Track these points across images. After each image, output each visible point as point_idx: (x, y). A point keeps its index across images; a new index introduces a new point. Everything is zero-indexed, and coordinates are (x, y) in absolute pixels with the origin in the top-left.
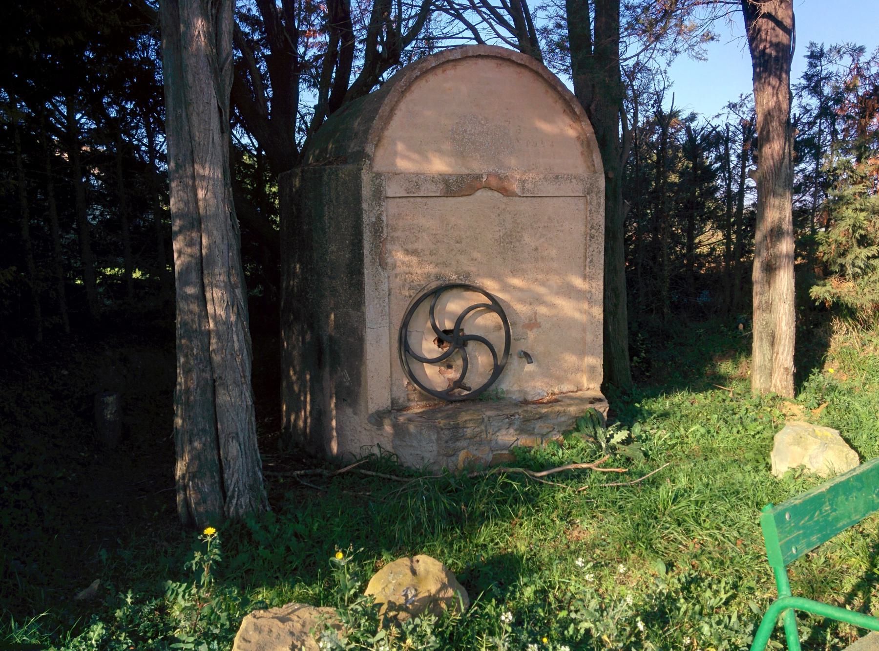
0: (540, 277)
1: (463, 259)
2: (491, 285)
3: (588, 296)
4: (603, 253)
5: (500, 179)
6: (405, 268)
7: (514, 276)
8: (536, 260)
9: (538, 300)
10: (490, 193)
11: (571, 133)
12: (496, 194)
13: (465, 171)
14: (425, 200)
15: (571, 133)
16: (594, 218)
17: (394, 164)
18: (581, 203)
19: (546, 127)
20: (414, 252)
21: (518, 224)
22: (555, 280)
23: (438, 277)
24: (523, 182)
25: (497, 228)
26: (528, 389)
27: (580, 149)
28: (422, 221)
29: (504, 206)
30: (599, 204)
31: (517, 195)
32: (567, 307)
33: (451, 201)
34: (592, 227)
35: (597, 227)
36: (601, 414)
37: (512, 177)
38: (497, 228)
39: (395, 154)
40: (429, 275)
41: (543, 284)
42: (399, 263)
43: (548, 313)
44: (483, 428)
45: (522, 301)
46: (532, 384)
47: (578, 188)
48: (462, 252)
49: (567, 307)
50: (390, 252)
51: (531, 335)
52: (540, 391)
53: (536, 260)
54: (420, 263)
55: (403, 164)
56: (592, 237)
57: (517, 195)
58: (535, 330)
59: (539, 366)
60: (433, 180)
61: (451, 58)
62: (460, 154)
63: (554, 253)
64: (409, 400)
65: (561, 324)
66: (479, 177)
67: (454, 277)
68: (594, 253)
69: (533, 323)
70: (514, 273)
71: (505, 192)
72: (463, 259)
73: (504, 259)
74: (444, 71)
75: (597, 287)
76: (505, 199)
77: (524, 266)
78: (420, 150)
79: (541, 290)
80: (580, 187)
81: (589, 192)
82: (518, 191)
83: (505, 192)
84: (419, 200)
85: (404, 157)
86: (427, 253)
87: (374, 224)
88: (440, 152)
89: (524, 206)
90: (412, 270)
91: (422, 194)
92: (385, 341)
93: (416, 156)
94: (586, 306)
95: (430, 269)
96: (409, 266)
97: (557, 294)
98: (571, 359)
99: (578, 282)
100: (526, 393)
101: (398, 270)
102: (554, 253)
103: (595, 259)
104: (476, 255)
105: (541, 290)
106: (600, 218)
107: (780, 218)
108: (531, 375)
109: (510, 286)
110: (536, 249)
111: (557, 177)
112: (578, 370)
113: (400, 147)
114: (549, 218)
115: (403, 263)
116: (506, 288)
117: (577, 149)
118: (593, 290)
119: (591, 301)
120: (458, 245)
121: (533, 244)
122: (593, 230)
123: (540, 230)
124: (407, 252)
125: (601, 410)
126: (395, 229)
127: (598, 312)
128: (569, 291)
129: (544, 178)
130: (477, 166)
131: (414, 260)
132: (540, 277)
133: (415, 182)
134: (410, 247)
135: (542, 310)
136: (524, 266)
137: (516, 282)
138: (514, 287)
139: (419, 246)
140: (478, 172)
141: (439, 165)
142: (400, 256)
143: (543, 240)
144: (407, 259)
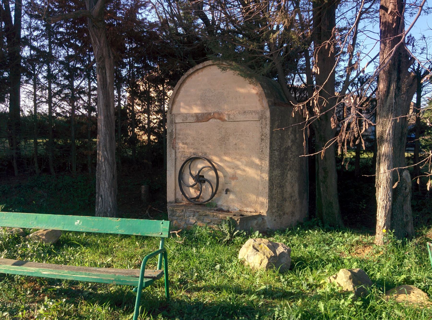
0: (238, 157)
1: (204, 147)
2: (215, 159)
3: (260, 168)
4: (268, 148)
5: (219, 114)
6: (182, 150)
7: (225, 156)
8: (236, 149)
9: (237, 167)
10: (216, 120)
11: (254, 91)
12: (218, 120)
13: (205, 112)
14: (190, 124)
15: (254, 91)
16: (264, 130)
17: (180, 111)
18: (258, 124)
19: (242, 90)
20: (186, 144)
21: (227, 133)
22: (244, 159)
23: (194, 154)
24: (229, 115)
25: (218, 135)
26: (231, 206)
27: (258, 98)
28: (188, 132)
29: (221, 126)
30: (266, 124)
31: (226, 121)
32: (251, 172)
33: (200, 124)
34: (262, 135)
35: (265, 135)
36: (236, 221)
37: (224, 113)
38: (218, 135)
39: (180, 107)
40: (191, 153)
41: (239, 160)
42: (180, 148)
43: (241, 174)
44: (183, 214)
45: (229, 167)
46: (233, 204)
47: (256, 117)
48: (203, 144)
49: (251, 172)
50: (178, 143)
51: (233, 183)
52: (236, 208)
53: (236, 149)
54: (188, 148)
55: (183, 111)
56: (262, 140)
57: (226, 121)
58: (235, 180)
59: (236, 196)
60: (192, 116)
61: (198, 68)
62: (204, 105)
63: (244, 146)
64: (183, 200)
65: (247, 179)
66: (210, 114)
67: (201, 154)
68: (264, 147)
69: (234, 177)
70: (225, 154)
71: (223, 120)
72: (204, 147)
73: (221, 148)
74: (198, 73)
75: (266, 164)
76: (222, 123)
77: (230, 152)
78: (189, 104)
79: (239, 163)
80: (257, 116)
81: (261, 118)
82: (226, 119)
83: (221, 119)
84: (188, 123)
85: (184, 108)
86: (191, 144)
87: (170, 133)
88: (196, 105)
89: (230, 125)
90: (185, 151)
91: (188, 121)
92: (173, 176)
93: (187, 107)
94: (259, 172)
95: (192, 151)
96: (184, 149)
97: (246, 165)
98: (253, 197)
99: (257, 161)
100: (229, 208)
101: (180, 150)
102: (244, 146)
103: (264, 150)
104: (209, 146)
105: (239, 163)
106: (267, 131)
107: (383, 131)
108: (233, 200)
109: (224, 160)
110: (236, 144)
111: (245, 112)
112: (256, 202)
113: (182, 104)
114: (242, 131)
115: (182, 147)
116: (222, 160)
117: (257, 99)
118: (263, 165)
119: (262, 171)
120: (202, 141)
121: (234, 142)
122: (263, 137)
123: (238, 136)
124: (183, 143)
125: (236, 219)
126: (179, 135)
127: (266, 176)
128: (252, 165)
129: (239, 113)
130: (211, 110)
131: (186, 146)
132: (238, 157)
133: (185, 117)
134: (184, 141)
135: (239, 172)
136: (230, 152)
137: (226, 158)
138: (225, 161)
139: (188, 141)
140: (210, 112)
141: (196, 110)
142: (181, 145)
143: (239, 140)
144: (183, 146)
